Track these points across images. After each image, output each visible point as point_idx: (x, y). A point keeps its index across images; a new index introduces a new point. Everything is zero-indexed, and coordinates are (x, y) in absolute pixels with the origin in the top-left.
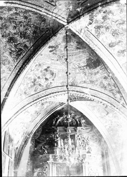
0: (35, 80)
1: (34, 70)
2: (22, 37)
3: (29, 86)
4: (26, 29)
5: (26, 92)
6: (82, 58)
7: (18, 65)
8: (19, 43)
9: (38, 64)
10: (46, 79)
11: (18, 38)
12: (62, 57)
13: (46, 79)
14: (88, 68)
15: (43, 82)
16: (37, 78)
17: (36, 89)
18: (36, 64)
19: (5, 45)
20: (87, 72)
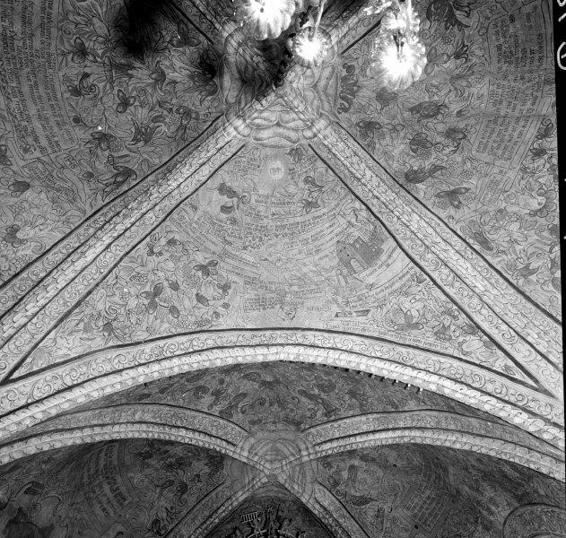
0: (157, 291)
1: (160, 253)
2: (138, 141)
3: (133, 303)
4: (155, 120)
5: (115, 324)
6: (322, 241)
7: (105, 210)
8: (126, 156)
9: (177, 237)
10: (200, 298)
11: (127, 143)
12: (261, 238)
13: (200, 298)
14: (345, 271)
15: (187, 303)
16: (166, 284)
17: (159, 321)
18: (171, 236)
19: (77, 147)
20: (343, 284)
